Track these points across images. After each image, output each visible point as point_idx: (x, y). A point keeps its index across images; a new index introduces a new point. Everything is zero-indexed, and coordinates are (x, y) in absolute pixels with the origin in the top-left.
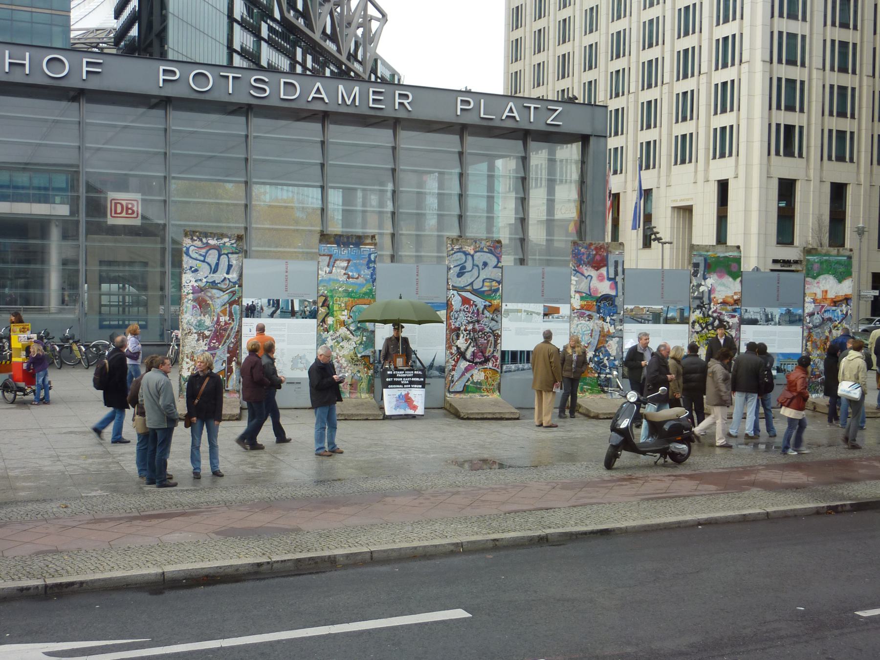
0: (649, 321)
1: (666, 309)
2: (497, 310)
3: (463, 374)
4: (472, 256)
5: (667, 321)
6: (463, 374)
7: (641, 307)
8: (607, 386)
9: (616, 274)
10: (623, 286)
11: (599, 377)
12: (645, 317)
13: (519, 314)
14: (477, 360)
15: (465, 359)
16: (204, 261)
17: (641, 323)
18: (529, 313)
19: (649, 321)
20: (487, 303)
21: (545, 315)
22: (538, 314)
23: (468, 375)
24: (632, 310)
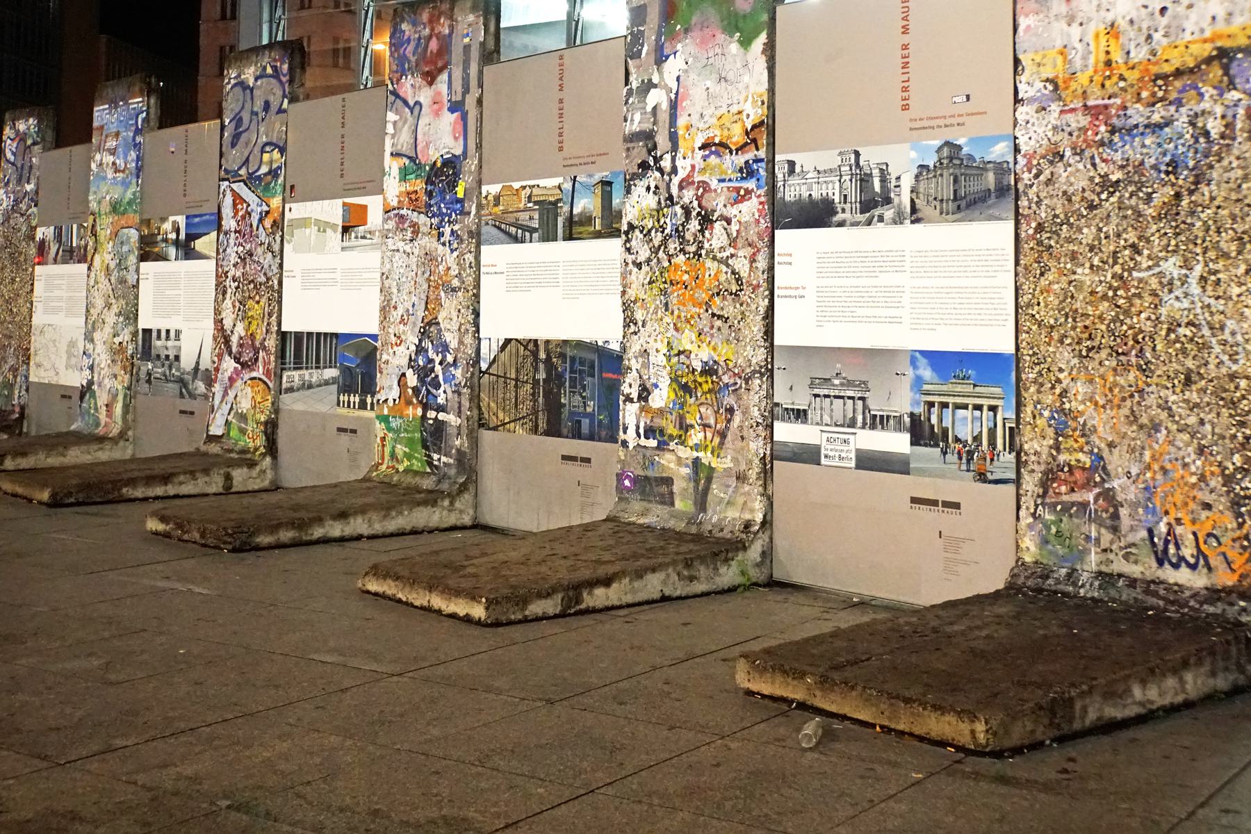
0: (532, 231)
1: (568, 186)
2: (278, 225)
3: (225, 394)
4: (252, 90)
5: (575, 229)
6: (225, 394)
7: (516, 185)
8: (439, 452)
9: (466, 90)
10: (480, 119)
11: (424, 417)
12: (524, 217)
13: (308, 231)
14: (245, 358)
15: (230, 354)
16: (13, 164)
17: (516, 240)
18: (323, 226)
19: (532, 231)
20: (265, 208)
21: (346, 230)
22: (333, 227)
23: (231, 394)
24: (497, 199)
